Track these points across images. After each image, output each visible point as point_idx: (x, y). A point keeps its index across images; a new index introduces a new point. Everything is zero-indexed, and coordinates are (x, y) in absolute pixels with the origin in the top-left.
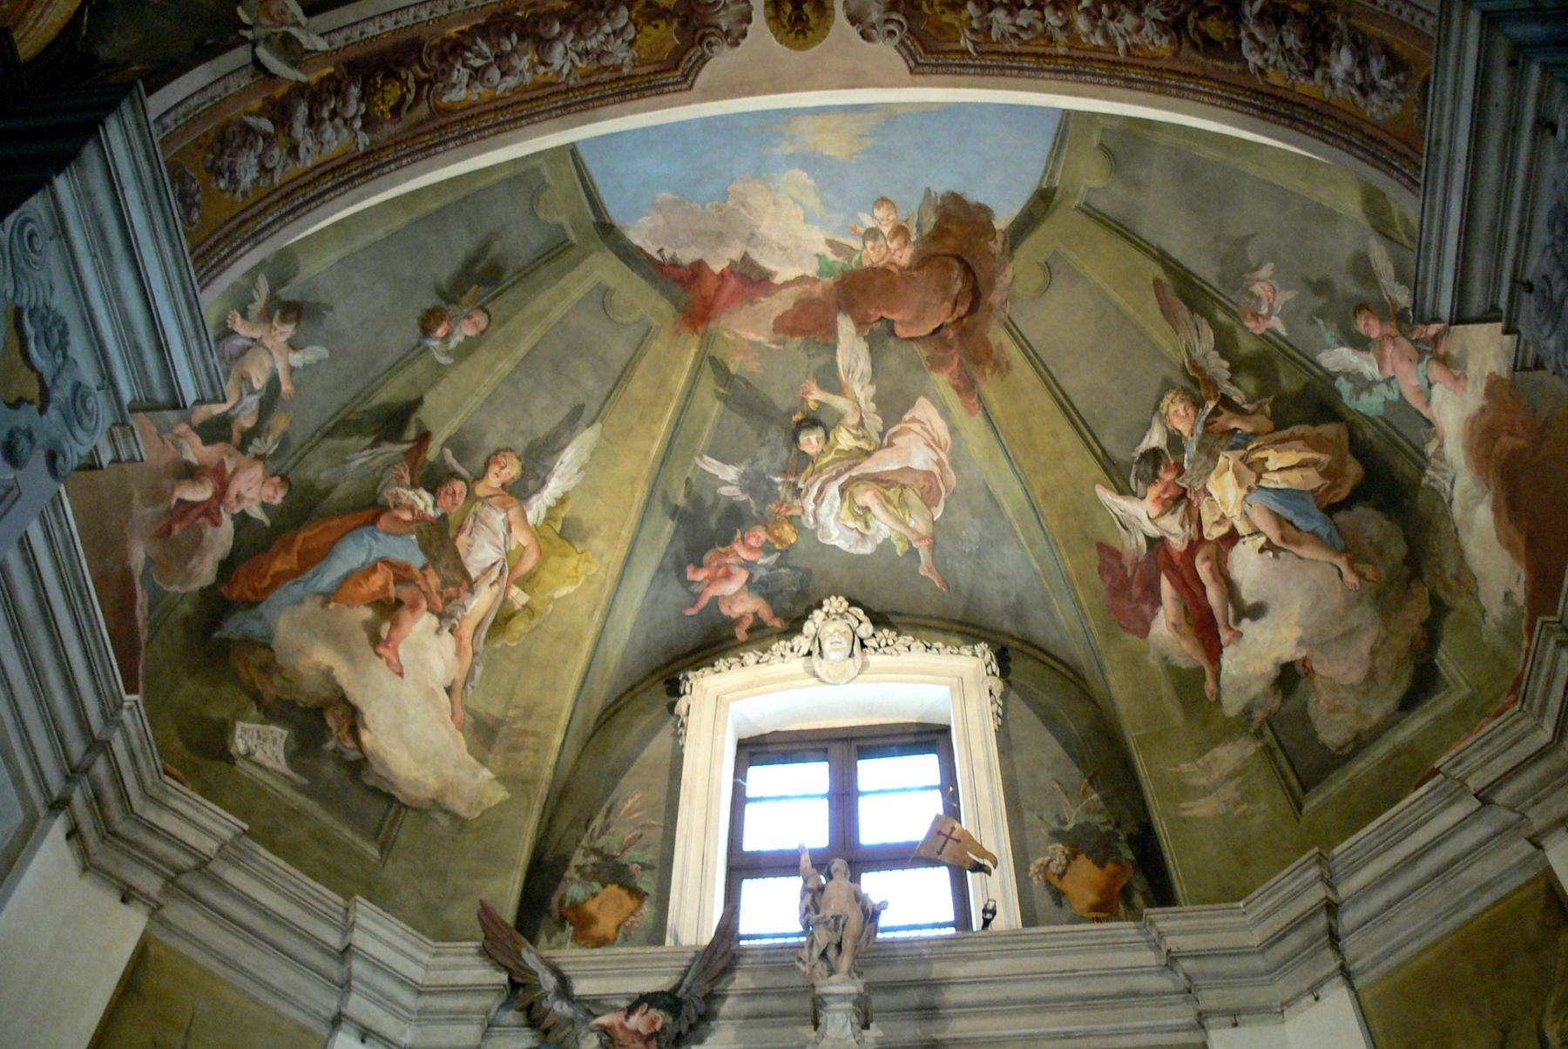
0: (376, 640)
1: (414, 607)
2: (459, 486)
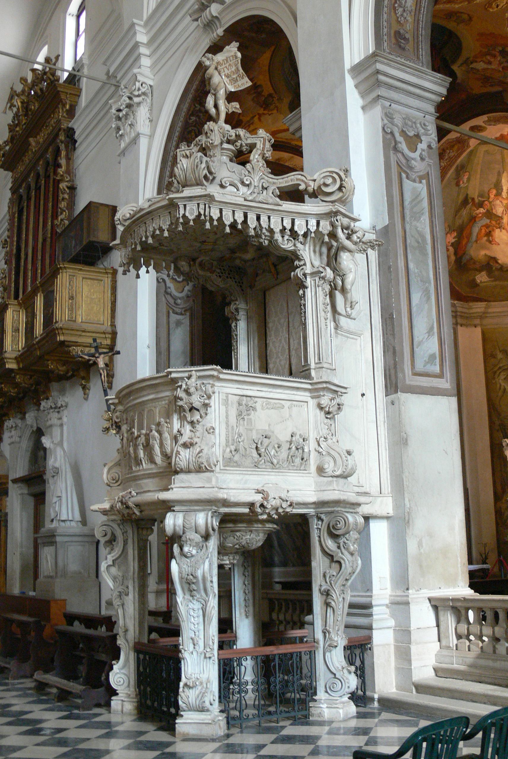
0: (490, 242)
1: (493, 230)
2: (486, 202)
